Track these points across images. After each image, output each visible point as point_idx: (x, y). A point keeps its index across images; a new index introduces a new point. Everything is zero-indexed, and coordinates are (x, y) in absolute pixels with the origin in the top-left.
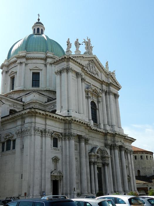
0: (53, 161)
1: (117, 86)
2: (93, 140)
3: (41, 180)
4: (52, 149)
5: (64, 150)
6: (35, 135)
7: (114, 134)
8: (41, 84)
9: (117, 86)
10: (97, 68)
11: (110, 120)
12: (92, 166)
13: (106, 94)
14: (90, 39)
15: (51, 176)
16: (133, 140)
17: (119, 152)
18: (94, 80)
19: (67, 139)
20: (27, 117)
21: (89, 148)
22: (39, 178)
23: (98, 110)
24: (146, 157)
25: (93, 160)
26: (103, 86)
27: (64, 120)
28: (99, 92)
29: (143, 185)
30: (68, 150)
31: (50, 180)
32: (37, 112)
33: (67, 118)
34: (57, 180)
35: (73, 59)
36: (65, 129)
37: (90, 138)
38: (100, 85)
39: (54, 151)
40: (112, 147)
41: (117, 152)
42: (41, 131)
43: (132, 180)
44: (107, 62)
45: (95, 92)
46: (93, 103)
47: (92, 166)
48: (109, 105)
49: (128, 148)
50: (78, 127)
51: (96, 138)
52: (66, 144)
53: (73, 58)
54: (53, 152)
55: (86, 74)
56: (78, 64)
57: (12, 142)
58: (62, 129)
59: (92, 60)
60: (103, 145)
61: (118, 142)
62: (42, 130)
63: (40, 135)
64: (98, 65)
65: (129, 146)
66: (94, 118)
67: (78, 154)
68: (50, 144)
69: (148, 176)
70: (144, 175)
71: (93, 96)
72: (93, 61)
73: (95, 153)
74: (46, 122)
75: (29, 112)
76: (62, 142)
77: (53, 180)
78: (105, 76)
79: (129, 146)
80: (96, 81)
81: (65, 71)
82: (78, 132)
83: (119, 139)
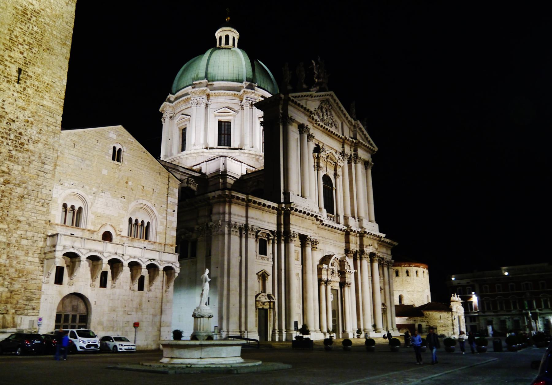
0: (258, 278)
1: (370, 146)
2: (325, 244)
4: (258, 257)
7: (361, 233)
8: (234, 141)
9: (370, 146)
10: (336, 113)
13: (349, 163)
15: (256, 301)
17: (370, 264)
18: (329, 135)
20: (216, 203)
21: (318, 256)
22: (237, 305)
24: (415, 273)
29: (407, 319)
31: (254, 307)
32: (233, 197)
34: (265, 308)
40: (358, 256)
41: (366, 263)
42: (240, 227)
43: (390, 312)
45: (331, 159)
46: (326, 178)
47: (323, 287)
49: (385, 257)
50: (300, 221)
51: (331, 240)
53: (293, 99)
55: (315, 125)
57: (190, 244)
59: (328, 100)
62: (242, 226)
68: (255, 249)
69: (417, 305)
70: (410, 303)
72: (329, 102)
75: (219, 196)
77: (259, 309)
80: (333, 138)
82: (301, 229)
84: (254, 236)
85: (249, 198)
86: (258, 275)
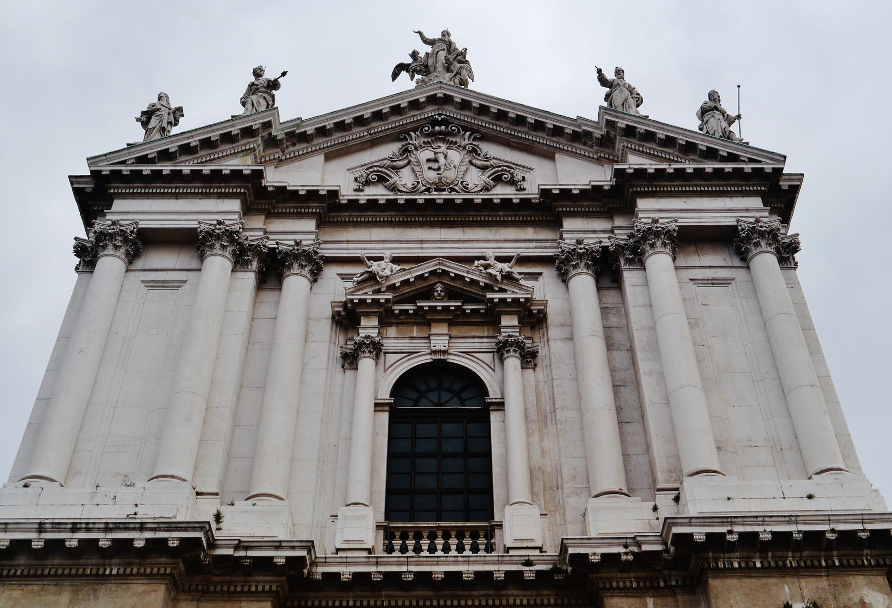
23: (494, 417)
26: (569, 224)
28: (482, 281)
44: (599, 71)
45: (451, 294)
64: (502, 128)
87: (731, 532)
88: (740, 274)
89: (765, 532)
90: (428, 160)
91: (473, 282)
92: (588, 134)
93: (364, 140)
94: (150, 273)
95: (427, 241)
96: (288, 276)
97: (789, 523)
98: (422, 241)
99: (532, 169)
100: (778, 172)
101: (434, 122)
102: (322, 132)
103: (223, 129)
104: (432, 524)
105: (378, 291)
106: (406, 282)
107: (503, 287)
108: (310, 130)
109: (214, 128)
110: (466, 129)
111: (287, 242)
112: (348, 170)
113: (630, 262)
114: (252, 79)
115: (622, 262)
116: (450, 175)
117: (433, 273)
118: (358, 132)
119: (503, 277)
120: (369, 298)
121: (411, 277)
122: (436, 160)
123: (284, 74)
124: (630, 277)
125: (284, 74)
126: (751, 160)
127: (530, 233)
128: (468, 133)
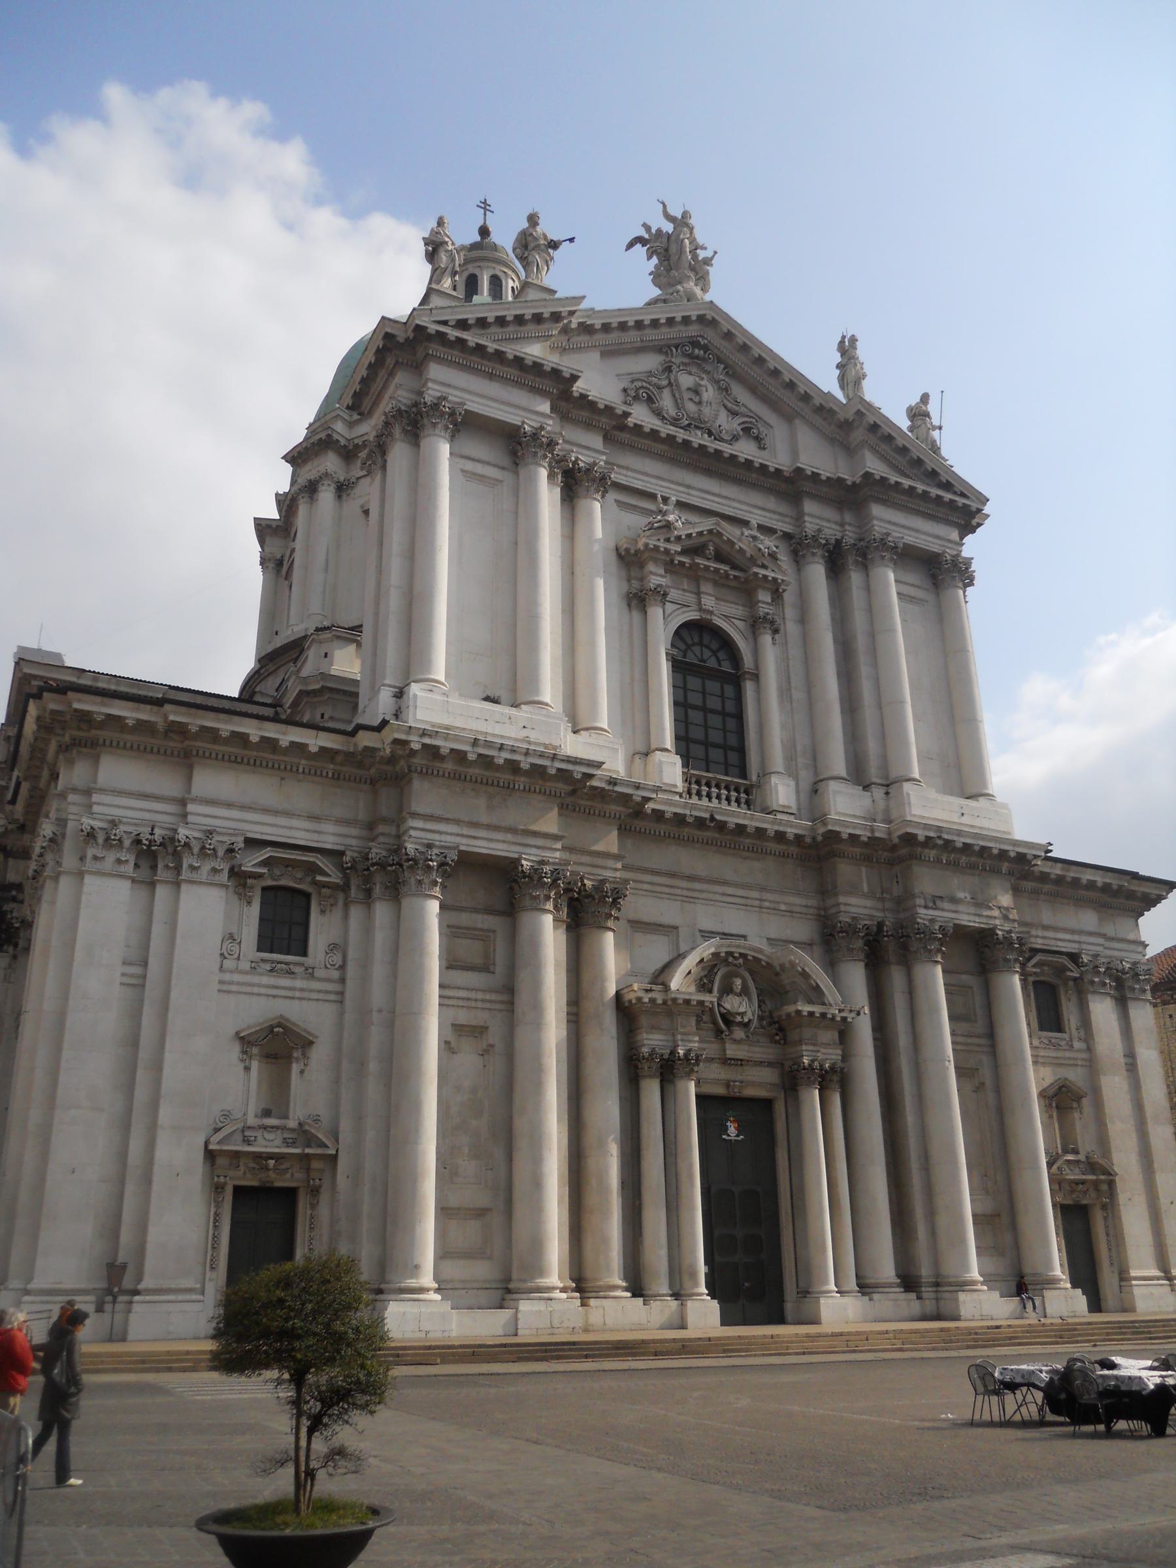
1: (948, 496)
3: (122, 1182)
4: (245, 965)
5: (351, 971)
6: (81, 875)
9: (948, 496)
11: (872, 747)
12: (651, 1091)
14: (686, 215)
15: (210, 1155)
16: (1152, 890)
18: (709, 472)
19: (377, 890)
23: (749, 687)
25: (652, 1041)
26: (809, 506)
27: (348, 755)
30: (379, 971)
32: (84, 717)
33: (365, 740)
35: (453, 333)
36: (371, 826)
37: (626, 881)
38: (783, 508)
39: (265, 980)
42: (138, 842)
45: (719, 557)
47: (651, 1091)
48: (861, 643)
51: (725, 883)
52: (368, 930)
54: (256, 990)
56: (512, 372)
58: (340, 821)
60: (803, 930)
61: (946, 905)
63: (129, 869)
65: (1104, 936)
66: (697, 733)
67: (983, 1041)
71: (706, 587)
73: (666, 988)
74: (189, 778)
76: (346, 917)
77: (239, 1191)
78: (832, 441)
79: (1104, 936)
81: (397, 431)
83: (960, 886)
84: (224, 877)
85: (172, 718)
86: (242, 1039)
87: (939, 837)
88: (930, 597)
89: (960, 841)
90: (689, 389)
91: (741, 550)
92: (831, 412)
93: (634, 345)
94: (467, 461)
95: (694, 488)
96: (586, 497)
97: (973, 838)
98: (689, 487)
99: (771, 427)
100: (979, 511)
101: (695, 344)
102: (606, 328)
103: (536, 307)
104: (710, 775)
105: (668, 540)
106: (689, 536)
107: (765, 563)
108: (598, 323)
109: (529, 304)
110: (720, 361)
111: (584, 459)
112: (618, 375)
113: (857, 562)
114: (526, 225)
115: (850, 562)
116: (706, 411)
117: (710, 531)
118: (632, 336)
119: (769, 554)
120: (662, 545)
121: (694, 531)
122: (697, 392)
123: (571, 240)
124: (855, 578)
125: (571, 240)
126: (963, 495)
127: (771, 503)
128: (722, 366)
